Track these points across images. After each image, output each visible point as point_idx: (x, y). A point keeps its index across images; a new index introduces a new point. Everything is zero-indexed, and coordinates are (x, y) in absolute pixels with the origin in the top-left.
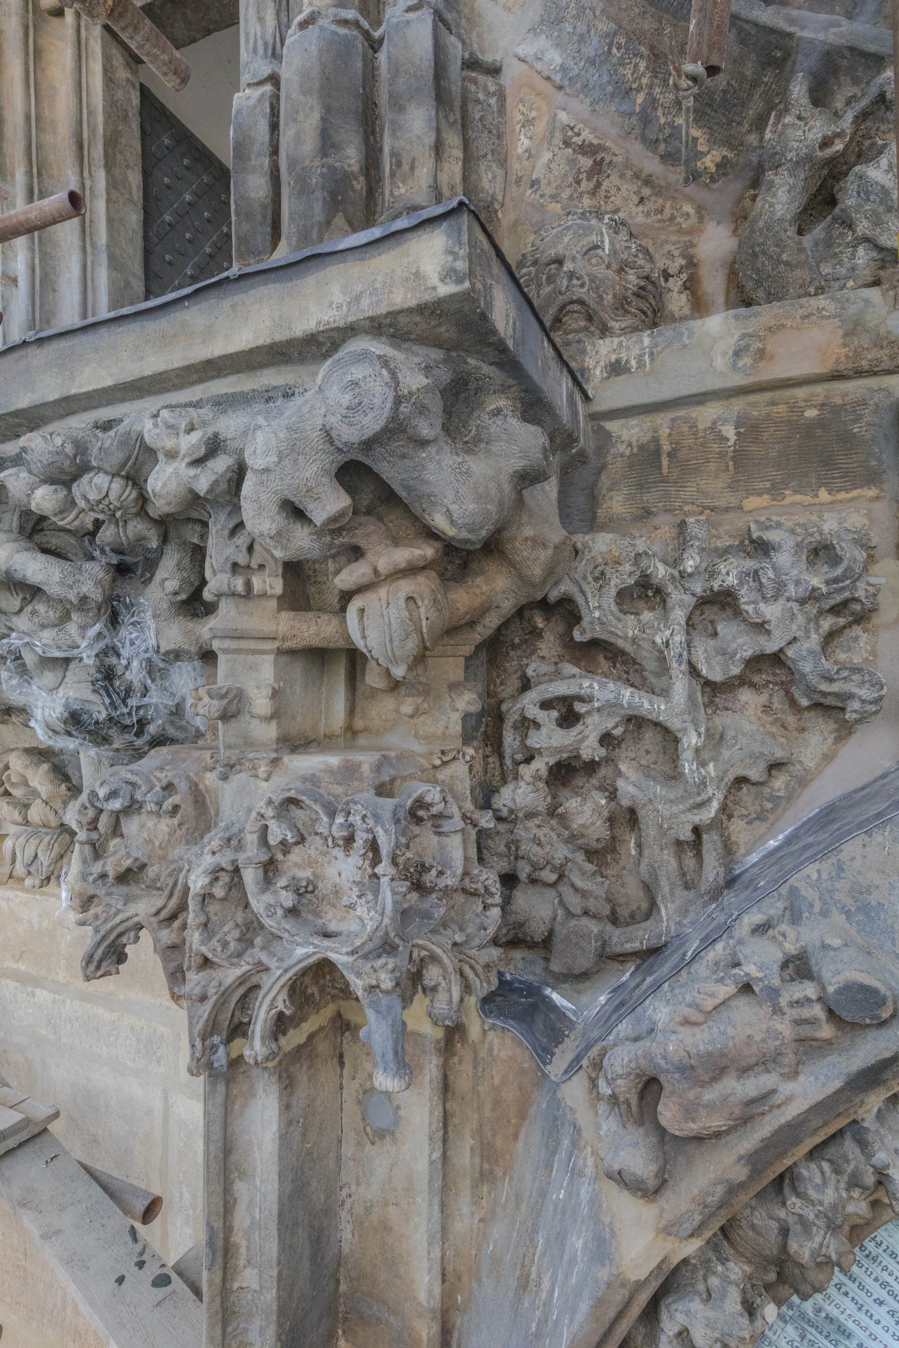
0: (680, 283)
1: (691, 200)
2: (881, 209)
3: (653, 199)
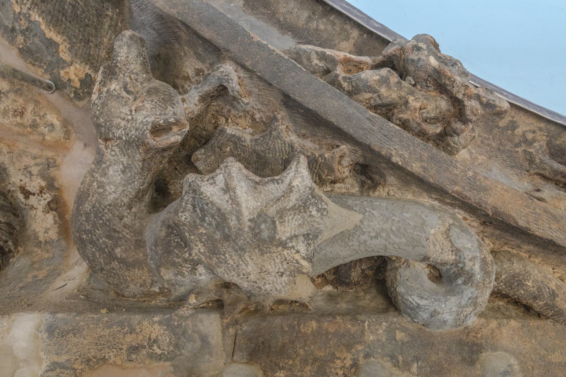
0: (44, 203)
1: (58, 111)
2: (218, 236)
3: (12, 96)
